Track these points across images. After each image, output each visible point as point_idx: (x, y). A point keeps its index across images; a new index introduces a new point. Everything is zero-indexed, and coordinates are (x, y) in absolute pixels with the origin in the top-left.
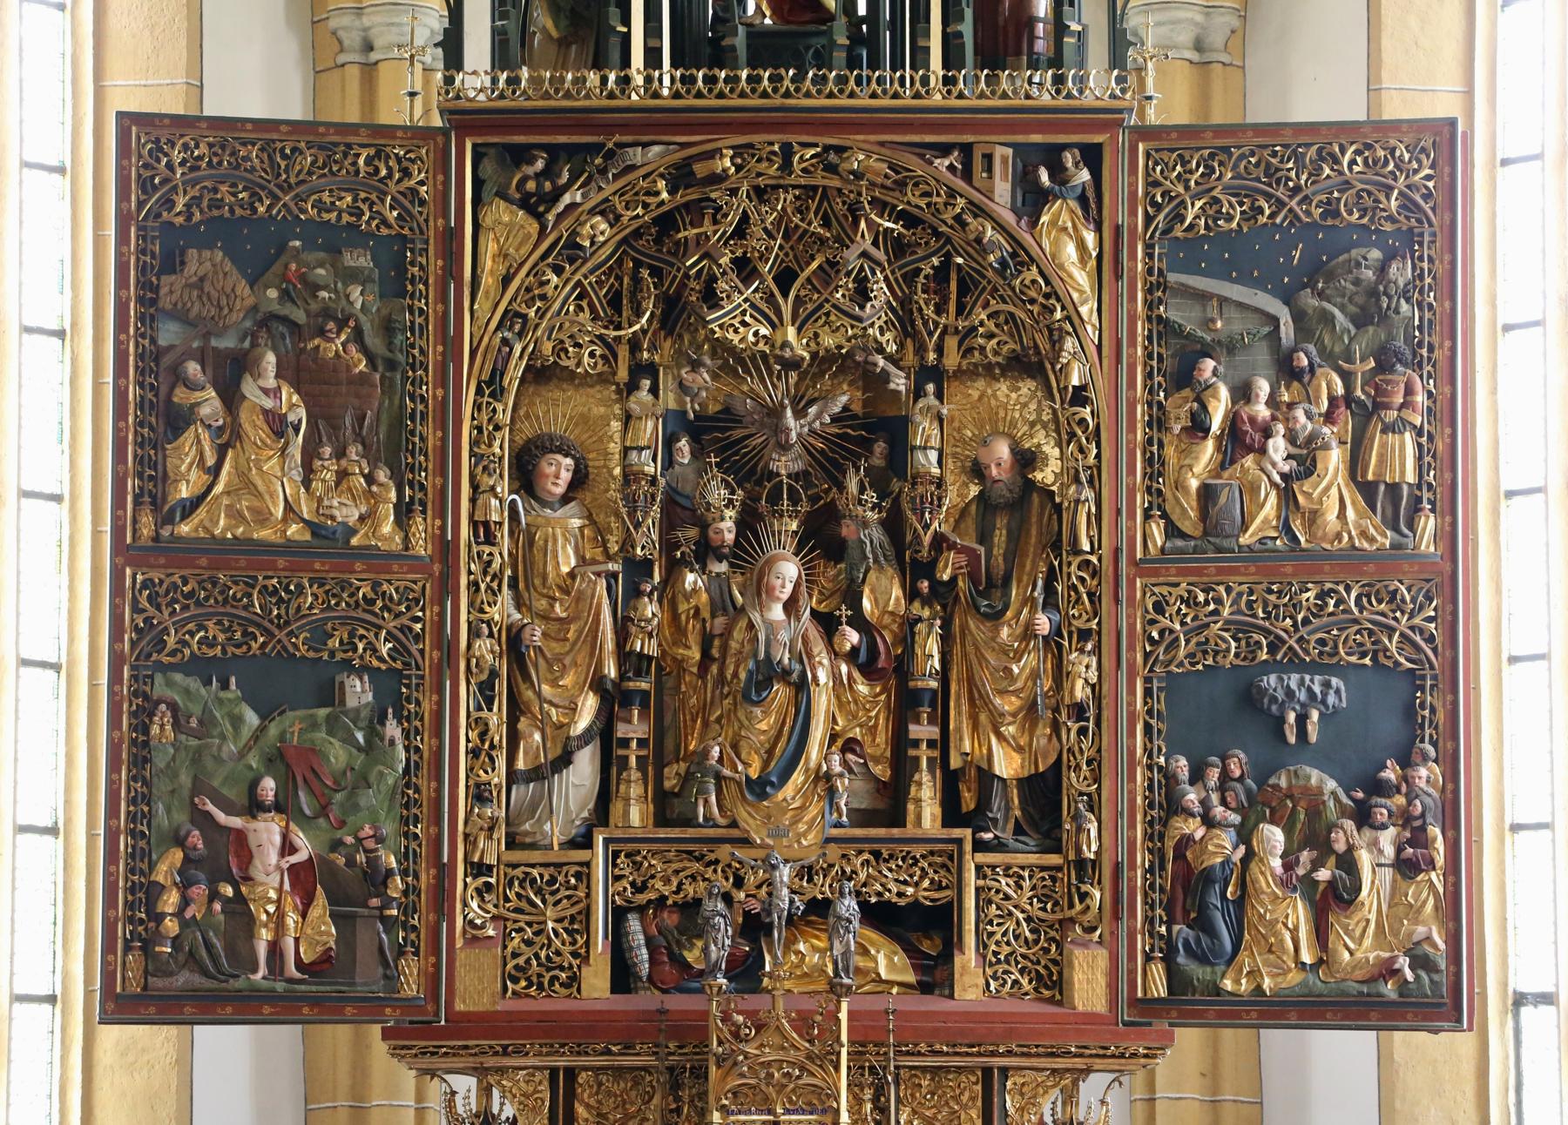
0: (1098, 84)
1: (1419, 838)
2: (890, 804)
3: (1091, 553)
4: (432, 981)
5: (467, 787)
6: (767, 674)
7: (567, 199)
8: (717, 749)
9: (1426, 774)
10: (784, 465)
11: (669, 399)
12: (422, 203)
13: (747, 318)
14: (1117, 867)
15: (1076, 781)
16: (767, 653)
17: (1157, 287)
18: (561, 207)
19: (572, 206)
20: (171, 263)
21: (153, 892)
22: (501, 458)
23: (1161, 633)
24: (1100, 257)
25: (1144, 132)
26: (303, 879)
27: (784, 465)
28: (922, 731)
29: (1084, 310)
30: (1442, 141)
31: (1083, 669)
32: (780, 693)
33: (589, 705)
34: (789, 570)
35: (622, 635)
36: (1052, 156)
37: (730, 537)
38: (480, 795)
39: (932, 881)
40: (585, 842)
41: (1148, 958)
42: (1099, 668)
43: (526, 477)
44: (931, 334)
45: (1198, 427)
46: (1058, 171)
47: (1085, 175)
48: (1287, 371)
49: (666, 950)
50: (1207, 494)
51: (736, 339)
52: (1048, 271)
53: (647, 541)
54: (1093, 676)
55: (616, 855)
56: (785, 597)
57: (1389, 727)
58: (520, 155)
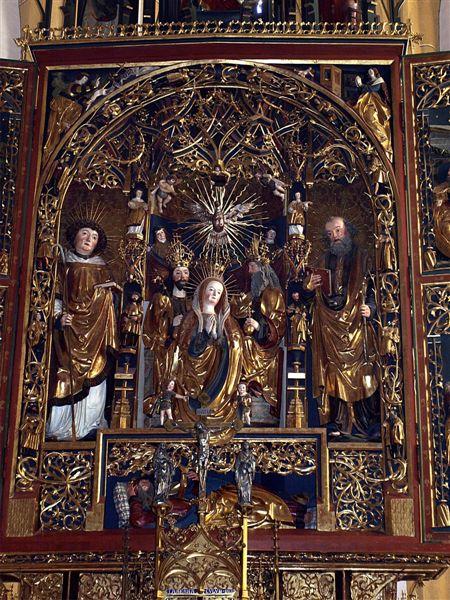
3: (393, 271)
5: (23, 405)
7: (98, 94)
8: (173, 382)
12: (20, 98)
13: (196, 156)
14: (417, 449)
16: (204, 330)
18: (94, 98)
19: (102, 97)
22: (56, 227)
23: (437, 312)
24: (391, 120)
29: (384, 144)
34: (217, 287)
36: (363, 71)
37: (186, 276)
39: (302, 461)
41: (438, 503)
42: (400, 334)
44: (299, 166)
46: (366, 79)
47: (381, 80)
51: (189, 166)
52: (363, 125)
53: (139, 273)
54: (397, 340)
55: (111, 445)
56: (216, 301)
58: (79, 74)
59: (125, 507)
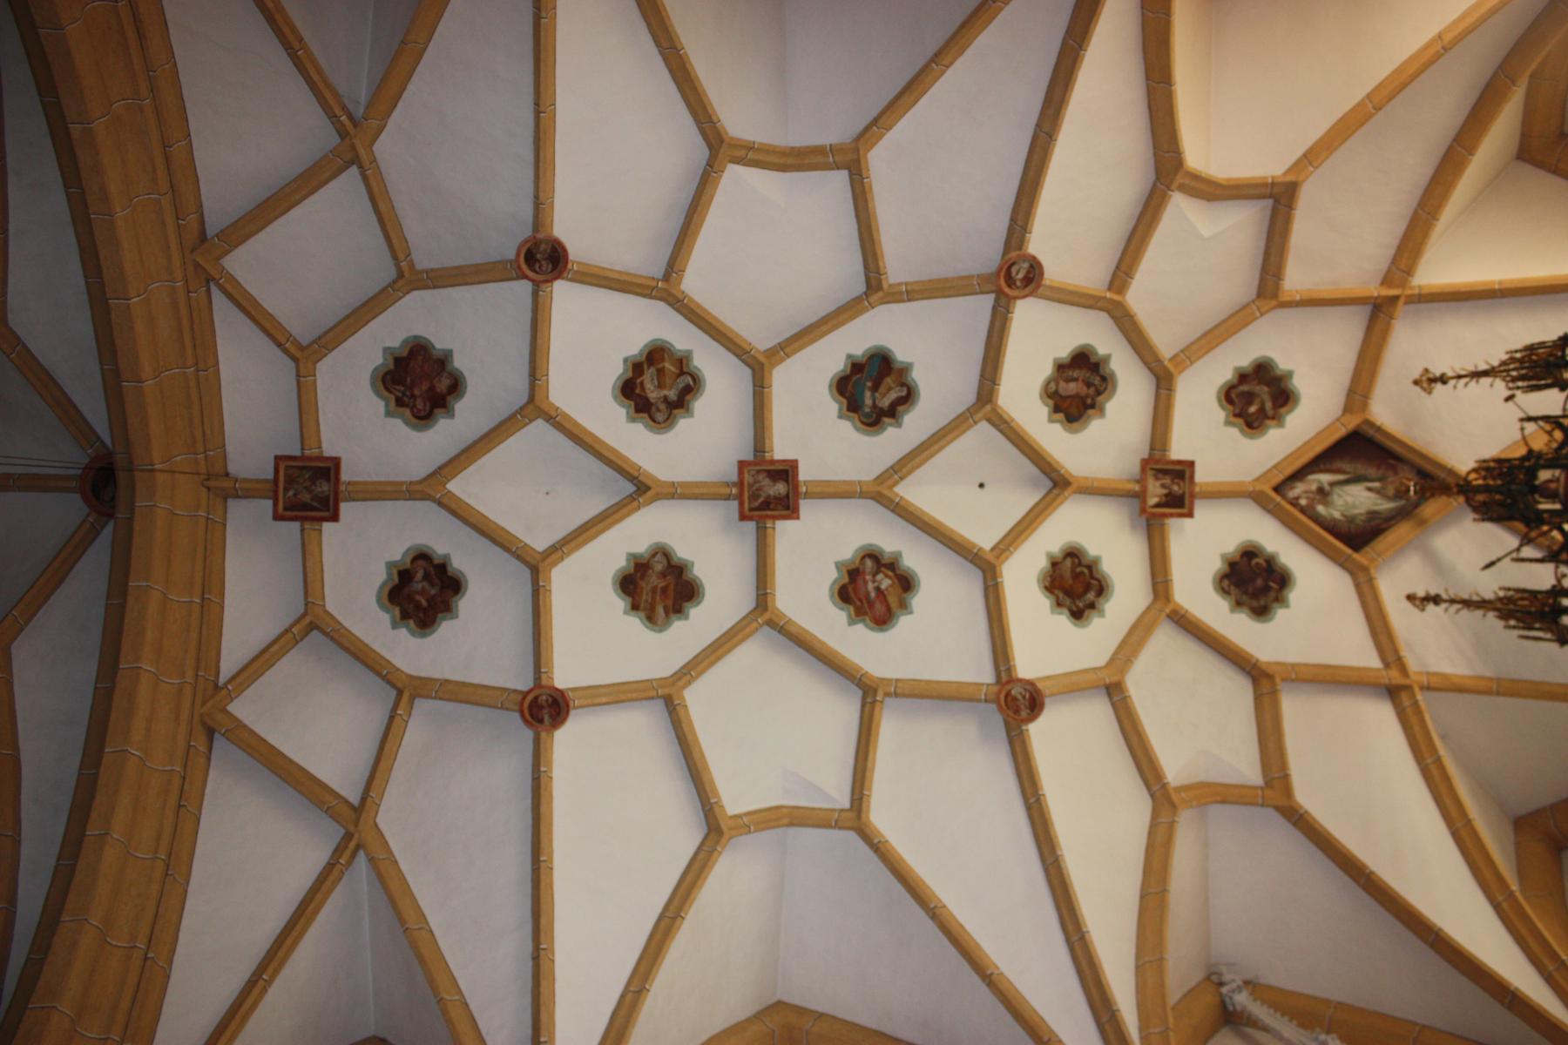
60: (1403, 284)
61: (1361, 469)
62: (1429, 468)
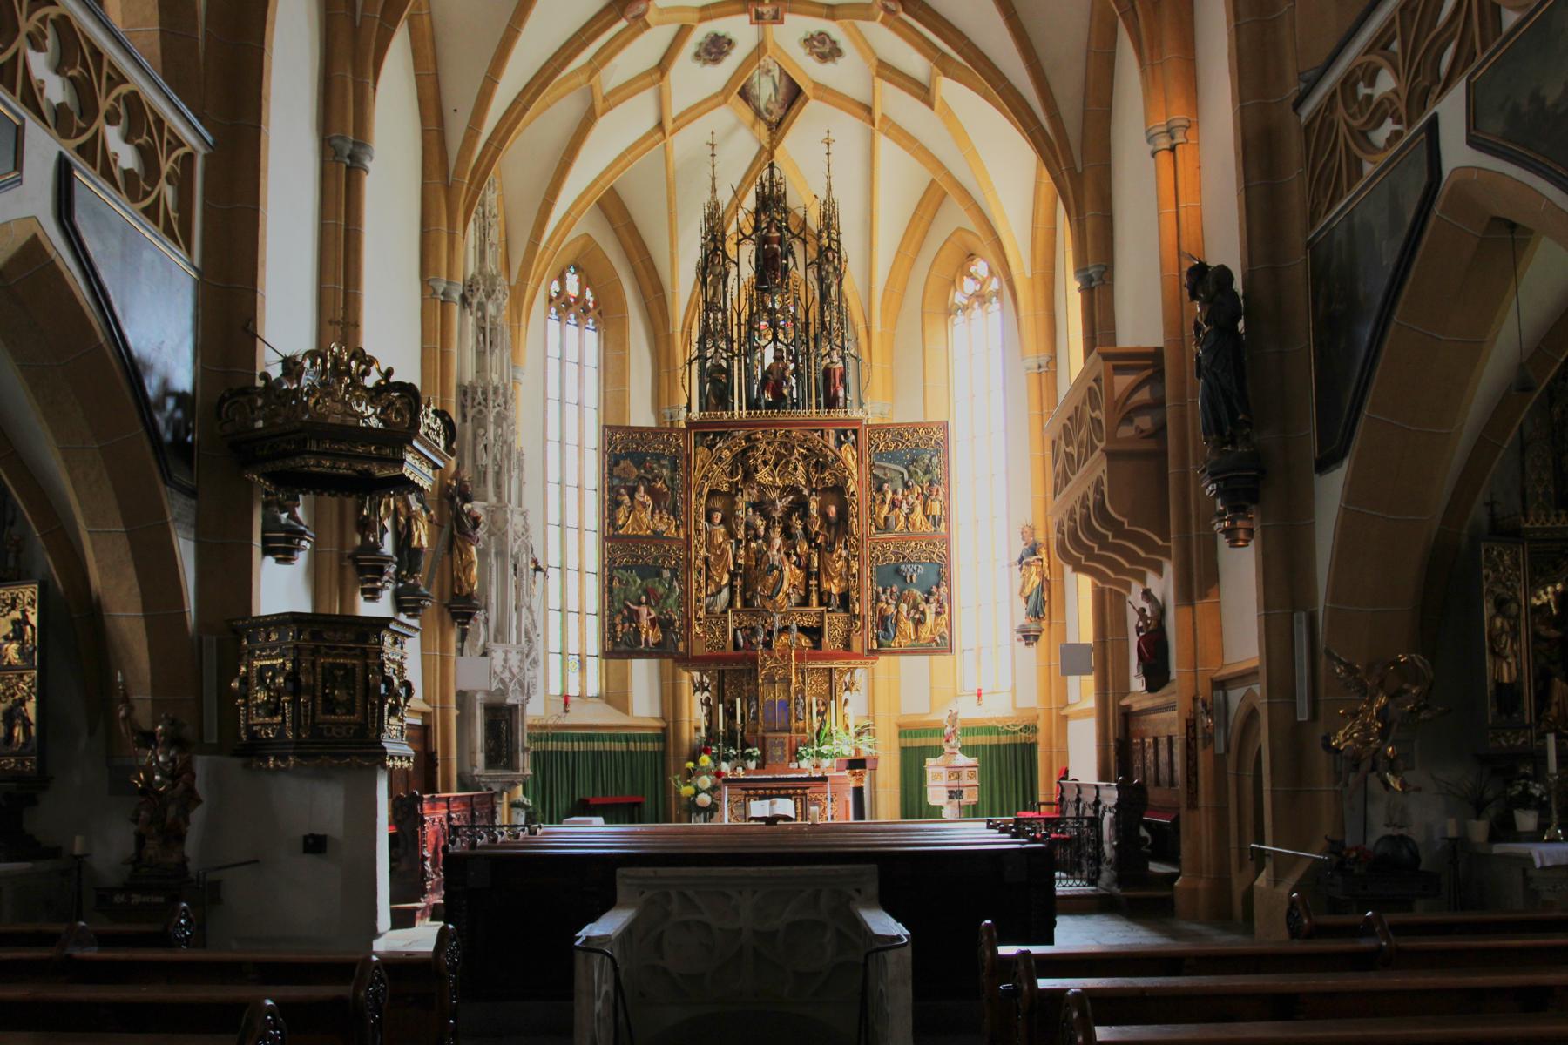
0: (855, 413)
1: (941, 606)
2: (805, 601)
4: (687, 647)
6: (772, 567)
9: (943, 590)
10: (776, 515)
11: (746, 498)
15: (853, 594)
17: (872, 465)
20: (617, 464)
21: (613, 626)
25: (868, 426)
26: (653, 622)
27: (776, 515)
28: (813, 582)
30: (945, 427)
31: (855, 565)
32: (776, 572)
33: (726, 578)
34: (778, 541)
35: (735, 557)
36: (845, 432)
38: (698, 600)
40: (725, 612)
43: (709, 519)
45: (883, 501)
46: (846, 437)
48: (906, 486)
49: (747, 638)
50: (886, 519)
53: (741, 534)
57: (934, 578)
58: (707, 434)
59: (741, 641)
60: (880, 130)
61: (783, 90)
62: (784, 126)
